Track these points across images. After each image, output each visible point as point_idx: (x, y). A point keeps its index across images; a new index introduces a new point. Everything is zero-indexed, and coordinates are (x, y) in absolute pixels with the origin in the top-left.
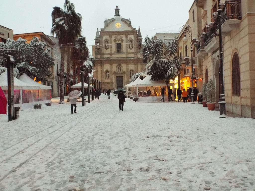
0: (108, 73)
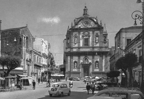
0: (77, 63)
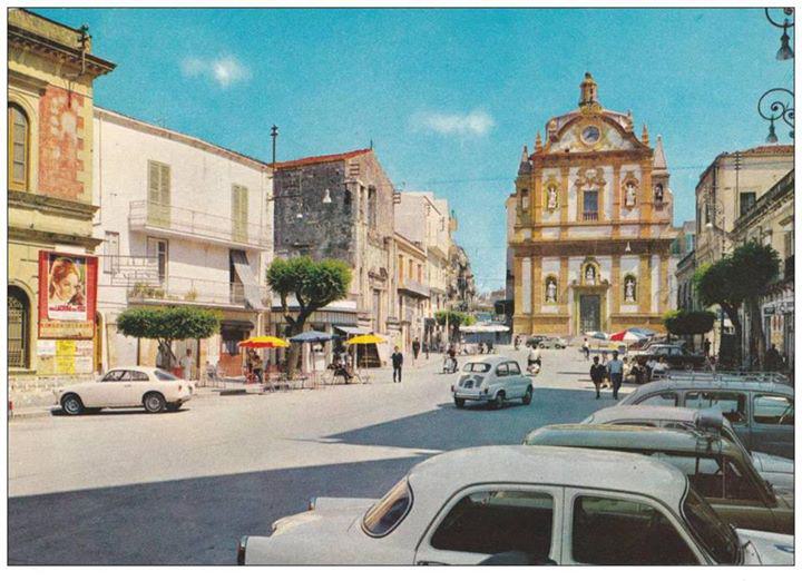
0: (555, 284)
